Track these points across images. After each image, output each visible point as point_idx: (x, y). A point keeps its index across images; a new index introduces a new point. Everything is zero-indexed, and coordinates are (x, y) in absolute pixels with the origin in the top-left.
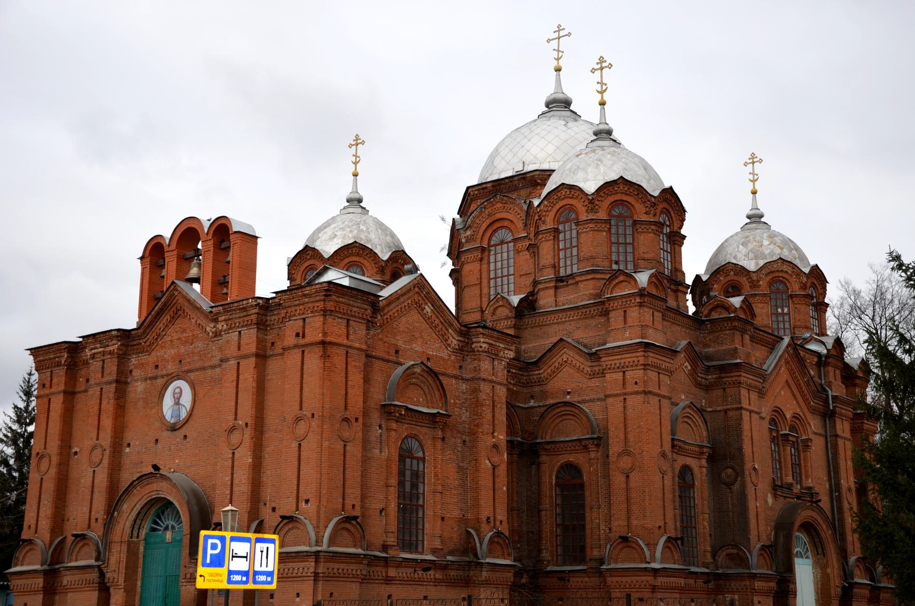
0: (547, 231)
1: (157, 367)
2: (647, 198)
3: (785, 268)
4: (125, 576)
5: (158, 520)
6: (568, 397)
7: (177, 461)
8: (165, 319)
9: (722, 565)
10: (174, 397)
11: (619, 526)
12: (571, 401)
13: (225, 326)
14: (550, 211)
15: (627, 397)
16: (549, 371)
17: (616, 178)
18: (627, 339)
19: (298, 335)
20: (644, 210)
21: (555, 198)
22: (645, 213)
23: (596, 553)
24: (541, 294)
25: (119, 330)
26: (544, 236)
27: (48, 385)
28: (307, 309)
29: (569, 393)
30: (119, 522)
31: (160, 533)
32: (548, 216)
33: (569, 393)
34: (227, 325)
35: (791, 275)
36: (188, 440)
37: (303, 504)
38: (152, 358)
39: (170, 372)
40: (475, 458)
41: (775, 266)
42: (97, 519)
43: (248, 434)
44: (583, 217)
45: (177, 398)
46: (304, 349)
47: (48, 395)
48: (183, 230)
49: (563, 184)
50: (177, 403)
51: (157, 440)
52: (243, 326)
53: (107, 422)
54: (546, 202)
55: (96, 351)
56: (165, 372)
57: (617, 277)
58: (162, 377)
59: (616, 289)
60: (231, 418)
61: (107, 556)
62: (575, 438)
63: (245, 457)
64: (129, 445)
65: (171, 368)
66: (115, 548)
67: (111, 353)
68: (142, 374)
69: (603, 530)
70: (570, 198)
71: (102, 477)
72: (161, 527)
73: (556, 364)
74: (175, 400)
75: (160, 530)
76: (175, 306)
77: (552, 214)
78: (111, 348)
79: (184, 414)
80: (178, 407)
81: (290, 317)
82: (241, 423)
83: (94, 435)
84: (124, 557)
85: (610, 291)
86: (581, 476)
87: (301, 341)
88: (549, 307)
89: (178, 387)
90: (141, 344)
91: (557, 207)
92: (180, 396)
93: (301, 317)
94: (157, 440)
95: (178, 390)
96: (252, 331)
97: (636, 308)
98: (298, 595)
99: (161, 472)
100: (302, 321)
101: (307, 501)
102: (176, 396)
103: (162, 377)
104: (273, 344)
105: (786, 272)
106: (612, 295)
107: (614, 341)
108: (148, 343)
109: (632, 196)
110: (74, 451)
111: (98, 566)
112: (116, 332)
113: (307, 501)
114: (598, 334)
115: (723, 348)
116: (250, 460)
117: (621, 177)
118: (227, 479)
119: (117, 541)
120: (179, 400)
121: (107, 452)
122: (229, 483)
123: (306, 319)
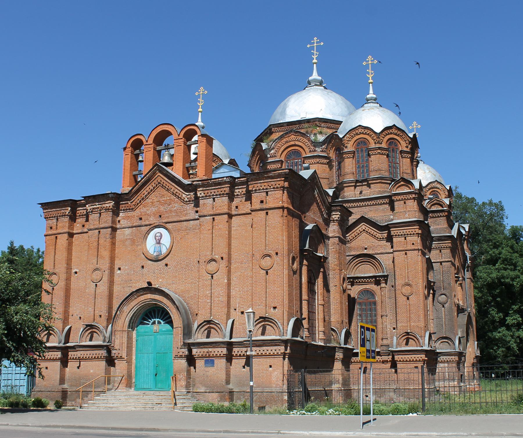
0: (349, 153)
1: (141, 219)
2: (407, 138)
3: (438, 186)
4: (127, 353)
5: (146, 318)
6: (366, 251)
7: (160, 280)
8: (148, 188)
9: (438, 348)
10: (156, 239)
11: (402, 326)
12: (368, 253)
13: (203, 194)
14: (350, 141)
15: (407, 252)
16: (353, 235)
17: (391, 125)
18: (406, 218)
19: (262, 202)
20: (405, 145)
21: (354, 133)
22: (406, 147)
23: (385, 342)
24: (345, 189)
25: (114, 193)
26: (347, 155)
27: (54, 228)
28: (270, 185)
29: (366, 249)
30: (120, 318)
31: (149, 326)
32: (349, 143)
33: (366, 249)
34: (204, 193)
35: (441, 190)
36: (169, 267)
37: (272, 309)
38: (137, 213)
39: (152, 222)
40: (335, 285)
41: (434, 184)
42: (100, 316)
43: (223, 264)
44: (373, 145)
45: (158, 240)
46: (267, 211)
47: (55, 234)
48: (158, 131)
49: (360, 126)
50: (159, 242)
51: (143, 267)
52: (217, 195)
53: (105, 254)
54: (348, 135)
55: (95, 206)
56: (147, 223)
57: (400, 182)
58: (146, 225)
59: (399, 189)
60: (209, 253)
61: (113, 339)
62: (371, 275)
63: (221, 277)
64: (120, 269)
65: (153, 220)
66: (118, 335)
67: (107, 209)
68: (129, 223)
69: (389, 328)
70: (364, 134)
71: (103, 287)
72: (150, 322)
73: (358, 231)
74: (156, 241)
75: (149, 324)
76: (156, 180)
77: (351, 143)
78: (108, 205)
79: (164, 251)
80: (159, 245)
81: (256, 190)
82: (217, 257)
83: (95, 261)
84: (125, 340)
85: (395, 190)
86: (374, 298)
87: (264, 206)
88: (351, 197)
89: (158, 233)
90: (128, 203)
91: (355, 138)
92: (161, 239)
93: (265, 191)
94: (143, 267)
95: (158, 235)
96: (224, 198)
97: (412, 200)
98: (271, 366)
99: (153, 286)
100: (265, 193)
101: (275, 308)
102: (157, 238)
103: (146, 225)
104: (237, 207)
105: (439, 188)
106: (396, 192)
107: (398, 219)
108: (134, 203)
109: (399, 136)
110: (74, 271)
111: (107, 346)
112: (112, 195)
113: (275, 308)
114: (384, 214)
115: (439, 227)
116: (226, 281)
117: (394, 124)
118: (208, 292)
119: (119, 330)
120: (160, 241)
121: (107, 272)
122: (210, 295)
123: (269, 192)
